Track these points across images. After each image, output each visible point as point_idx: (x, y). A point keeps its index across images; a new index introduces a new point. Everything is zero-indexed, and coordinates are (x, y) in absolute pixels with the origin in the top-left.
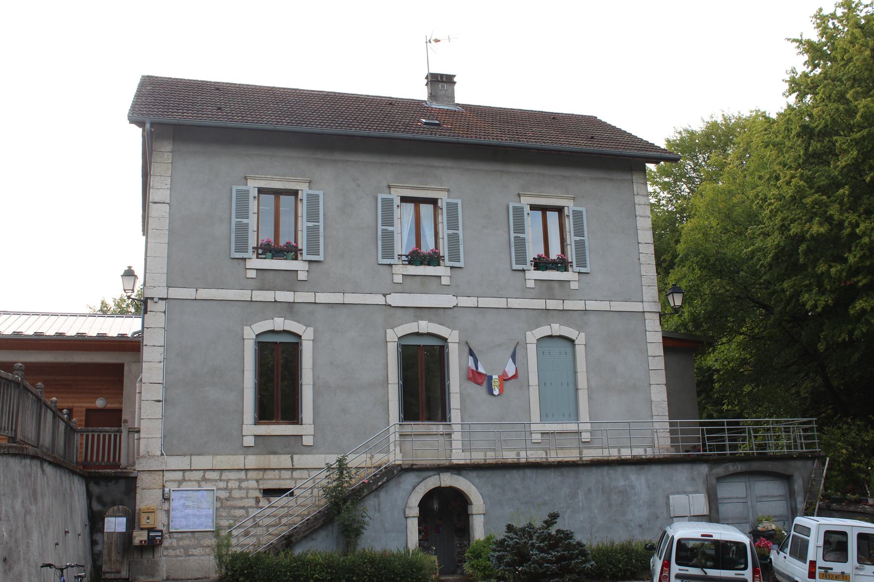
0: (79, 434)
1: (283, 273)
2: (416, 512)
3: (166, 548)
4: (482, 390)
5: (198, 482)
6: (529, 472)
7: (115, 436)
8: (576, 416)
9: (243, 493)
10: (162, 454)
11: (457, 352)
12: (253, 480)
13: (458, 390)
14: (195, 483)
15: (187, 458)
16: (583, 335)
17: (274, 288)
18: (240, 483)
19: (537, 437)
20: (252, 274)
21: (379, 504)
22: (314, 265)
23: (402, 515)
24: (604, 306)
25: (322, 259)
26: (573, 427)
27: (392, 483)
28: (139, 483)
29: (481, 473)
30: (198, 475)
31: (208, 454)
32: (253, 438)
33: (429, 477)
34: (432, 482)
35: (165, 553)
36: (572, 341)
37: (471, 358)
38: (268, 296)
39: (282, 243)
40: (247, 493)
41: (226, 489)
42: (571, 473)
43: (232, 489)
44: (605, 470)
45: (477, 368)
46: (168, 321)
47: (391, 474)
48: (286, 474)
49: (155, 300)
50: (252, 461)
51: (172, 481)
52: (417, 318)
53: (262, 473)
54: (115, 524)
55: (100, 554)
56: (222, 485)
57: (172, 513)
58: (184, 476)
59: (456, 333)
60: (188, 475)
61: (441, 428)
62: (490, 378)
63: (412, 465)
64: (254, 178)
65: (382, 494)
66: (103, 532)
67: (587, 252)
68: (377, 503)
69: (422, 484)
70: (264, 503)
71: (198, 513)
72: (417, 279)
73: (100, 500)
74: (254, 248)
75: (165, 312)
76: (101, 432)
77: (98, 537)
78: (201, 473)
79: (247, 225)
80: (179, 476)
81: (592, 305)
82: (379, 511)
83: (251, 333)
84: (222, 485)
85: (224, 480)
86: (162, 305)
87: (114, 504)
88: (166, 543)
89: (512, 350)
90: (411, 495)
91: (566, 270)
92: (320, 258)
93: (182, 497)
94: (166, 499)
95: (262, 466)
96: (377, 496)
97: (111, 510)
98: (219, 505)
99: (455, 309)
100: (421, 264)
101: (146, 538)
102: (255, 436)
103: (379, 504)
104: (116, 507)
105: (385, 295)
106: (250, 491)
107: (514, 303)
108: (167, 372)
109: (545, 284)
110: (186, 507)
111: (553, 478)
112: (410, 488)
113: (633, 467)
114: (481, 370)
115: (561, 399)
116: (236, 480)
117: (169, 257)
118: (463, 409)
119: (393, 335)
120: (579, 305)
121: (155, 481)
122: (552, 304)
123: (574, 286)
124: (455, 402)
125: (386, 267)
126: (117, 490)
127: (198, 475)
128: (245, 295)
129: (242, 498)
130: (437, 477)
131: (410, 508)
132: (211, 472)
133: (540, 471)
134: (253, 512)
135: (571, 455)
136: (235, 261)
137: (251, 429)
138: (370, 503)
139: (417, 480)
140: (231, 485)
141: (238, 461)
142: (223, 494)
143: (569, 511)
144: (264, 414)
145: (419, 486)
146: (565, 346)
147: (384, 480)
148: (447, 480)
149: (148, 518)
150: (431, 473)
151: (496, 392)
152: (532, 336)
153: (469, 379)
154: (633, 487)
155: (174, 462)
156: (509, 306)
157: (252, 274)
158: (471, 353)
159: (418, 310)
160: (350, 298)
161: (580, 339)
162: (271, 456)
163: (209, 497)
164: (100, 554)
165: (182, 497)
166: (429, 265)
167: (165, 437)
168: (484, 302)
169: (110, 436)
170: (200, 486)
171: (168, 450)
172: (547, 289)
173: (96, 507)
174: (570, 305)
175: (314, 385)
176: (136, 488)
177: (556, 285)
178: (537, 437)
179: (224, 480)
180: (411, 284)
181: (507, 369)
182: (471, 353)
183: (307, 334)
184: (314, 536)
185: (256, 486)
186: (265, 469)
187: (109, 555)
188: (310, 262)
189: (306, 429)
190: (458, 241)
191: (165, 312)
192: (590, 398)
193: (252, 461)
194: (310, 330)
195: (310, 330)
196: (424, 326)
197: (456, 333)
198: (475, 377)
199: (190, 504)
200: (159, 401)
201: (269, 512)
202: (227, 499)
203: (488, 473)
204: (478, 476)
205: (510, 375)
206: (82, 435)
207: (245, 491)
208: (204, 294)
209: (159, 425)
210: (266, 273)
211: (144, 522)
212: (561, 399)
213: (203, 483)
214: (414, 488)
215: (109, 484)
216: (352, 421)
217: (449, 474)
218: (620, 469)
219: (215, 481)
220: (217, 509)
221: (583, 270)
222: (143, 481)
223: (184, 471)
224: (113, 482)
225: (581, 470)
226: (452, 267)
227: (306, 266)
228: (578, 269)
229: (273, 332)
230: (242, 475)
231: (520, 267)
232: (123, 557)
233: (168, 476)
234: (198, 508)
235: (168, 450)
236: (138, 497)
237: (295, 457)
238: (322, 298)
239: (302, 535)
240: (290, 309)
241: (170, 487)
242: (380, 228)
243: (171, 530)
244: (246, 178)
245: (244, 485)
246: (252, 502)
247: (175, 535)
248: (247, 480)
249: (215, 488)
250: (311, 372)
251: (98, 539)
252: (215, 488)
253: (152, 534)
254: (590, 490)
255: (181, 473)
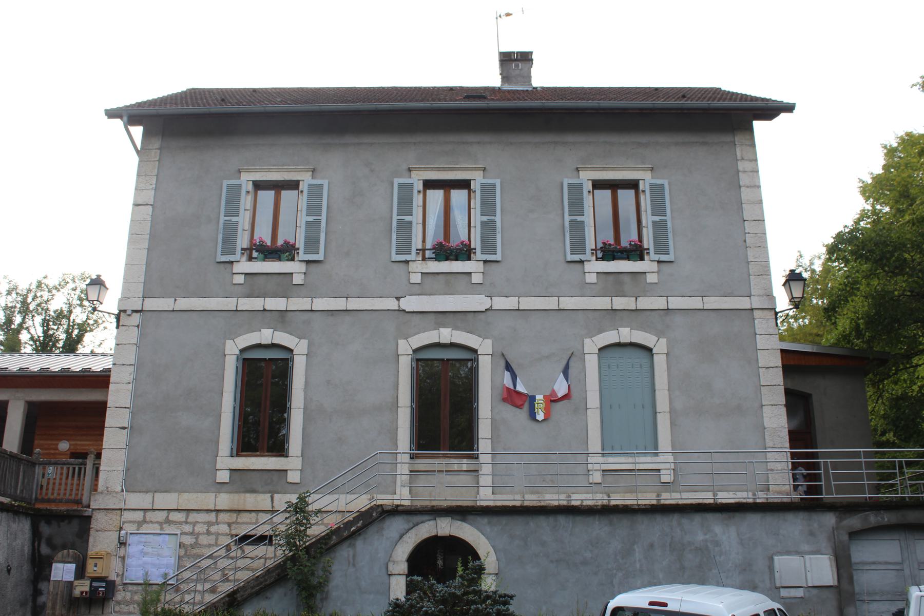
0: (41, 467)
1: (276, 276)
2: (403, 567)
3: (119, 603)
4: (521, 415)
5: (161, 524)
6: (562, 520)
7: (80, 469)
8: (653, 448)
9: (211, 540)
10: (122, 491)
11: (489, 366)
12: (224, 523)
13: (489, 415)
14: (157, 526)
15: (150, 495)
16: (663, 341)
17: (264, 295)
18: (209, 527)
19: (597, 477)
20: (240, 279)
21: (354, 556)
22: (313, 267)
23: (384, 570)
24: (695, 303)
25: (322, 258)
26: (646, 462)
27: (373, 529)
28: (94, 524)
29: (495, 519)
30: (161, 516)
31: (175, 491)
32: (228, 472)
33: (422, 522)
34: (427, 529)
35: (117, 609)
36: (650, 350)
37: (507, 375)
38: (256, 304)
39: (280, 242)
40: (217, 539)
41: (192, 534)
42: (623, 525)
43: (199, 534)
44: (675, 519)
45: (515, 386)
46: (142, 336)
47: (374, 517)
48: (265, 517)
49: (129, 312)
50: (224, 500)
51: (130, 522)
52: (438, 326)
53: (235, 515)
54: (63, 571)
55: (44, 606)
56: (188, 528)
57: (128, 561)
58: (144, 516)
59: (488, 342)
60: (149, 515)
61: (465, 464)
62: (533, 399)
63: (397, 506)
64: (248, 171)
65: (359, 543)
66: (49, 580)
67: (670, 236)
68: (351, 553)
69: (413, 531)
70: (235, 552)
71: (157, 562)
72: (441, 276)
73: (50, 543)
74: (242, 249)
75: (138, 326)
76: (64, 464)
77: (43, 586)
78: (165, 514)
79: (237, 223)
80: (139, 516)
81: (676, 303)
82: (354, 565)
83: (233, 348)
84: (188, 528)
85: (190, 523)
86: (136, 318)
87: (64, 547)
88: (119, 596)
89: (564, 363)
90: (399, 545)
91: (642, 259)
92: (320, 257)
93: (140, 542)
94: (122, 544)
95: (236, 508)
96: (353, 546)
97: (60, 555)
98: (182, 553)
99: (488, 312)
100: (447, 259)
101: (87, 589)
102: (231, 470)
103: (354, 556)
104: (66, 551)
105: (398, 299)
106: (220, 537)
107: (568, 303)
108: (136, 395)
109: (611, 278)
110: (145, 554)
111: (598, 528)
112: (397, 536)
113: (718, 515)
114: (520, 388)
115: (630, 424)
116: (204, 523)
117: (148, 264)
118: (495, 439)
119: (406, 348)
120: (659, 303)
121: (111, 522)
122: (620, 303)
123: (652, 278)
124: (484, 429)
125: (401, 264)
126: (69, 530)
127: (161, 516)
128: (229, 304)
129: (210, 546)
130: (432, 523)
131: (394, 562)
132: (176, 513)
133: (579, 519)
134: (223, 563)
135: (648, 498)
136: (222, 265)
137: (227, 462)
138: (344, 552)
139: (406, 526)
140: (200, 528)
141: (208, 500)
142: (188, 540)
143: (620, 574)
144: (247, 443)
145: (408, 535)
146: (639, 357)
147: (359, 525)
148: (445, 527)
149: (96, 566)
150: (426, 517)
151: (540, 416)
152: (592, 345)
153: (504, 400)
154: (717, 544)
155: (136, 500)
156: (561, 307)
157: (240, 279)
158: (508, 367)
159: (441, 316)
160: (355, 304)
161: (660, 347)
162: (248, 495)
163: (172, 543)
164: (44, 606)
165: (140, 542)
166: (457, 259)
167: (128, 470)
168: (527, 303)
169: (74, 469)
170: (162, 529)
171: (130, 486)
172: (614, 284)
173: (45, 550)
174: (645, 303)
175: (305, 409)
176: (89, 529)
177: (627, 279)
178: (597, 477)
179: (190, 523)
180: (431, 284)
181: (556, 388)
182: (508, 367)
183: (300, 347)
184: (268, 594)
185: (228, 531)
186: (240, 511)
187: (53, 608)
188: (308, 262)
189: (292, 463)
190: (495, 229)
191: (138, 326)
192: (673, 424)
193: (224, 500)
194: (304, 343)
195: (304, 343)
196: (446, 335)
197: (488, 342)
198: (512, 397)
199: (150, 550)
200: (124, 428)
201: (241, 563)
202: (192, 546)
203: (504, 520)
204: (489, 523)
205: (560, 395)
206: (62, 468)
207: (214, 537)
208: (184, 304)
209: (122, 455)
210: (256, 278)
211: (91, 570)
212: (630, 424)
213: (165, 526)
214: (401, 537)
215: (62, 524)
216: (354, 452)
217: (448, 519)
218: (698, 518)
219: (180, 523)
220: (180, 558)
221: (664, 258)
222: (99, 521)
223: (145, 510)
224: (66, 521)
225: (639, 518)
226: (485, 262)
227: (302, 267)
228: (657, 257)
229: (259, 346)
230: (212, 517)
231: (576, 257)
232: (69, 611)
233: (127, 516)
234: (158, 555)
235: (130, 486)
236: (91, 540)
237: (276, 496)
238: (321, 304)
239: (249, 591)
240: (281, 319)
241: (129, 528)
242: (395, 218)
243: (125, 582)
244: (239, 172)
245: (213, 529)
246: (223, 552)
247: (130, 588)
248: (217, 523)
249: (179, 532)
250: (302, 393)
251: (43, 588)
252: (179, 532)
253: (95, 584)
254: (652, 546)
255: (142, 513)
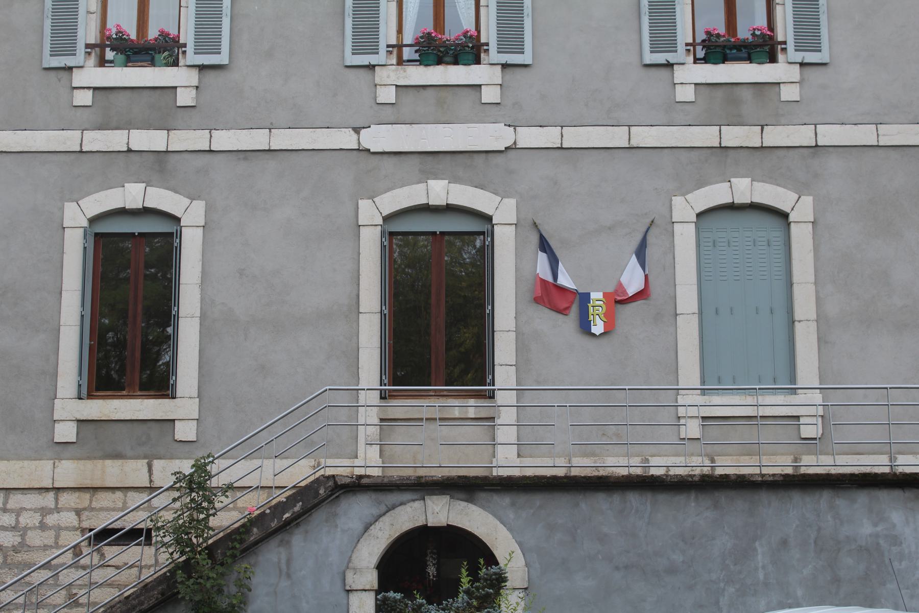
2: (371, 578)
4: (568, 324)
6: (634, 499)
8: (789, 381)
9: (48, 538)
11: (512, 243)
13: (512, 325)
16: (807, 201)
17: (128, 125)
18: (43, 516)
19: (693, 429)
20: (84, 98)
22: (211, 76)
24: (864, 135)
25: (226, 61)
26: (775, 404)
27: (319, 516)
29: (522, 498)
33: (402, 504)
34: (410, 515)
36: (784, 216)
37: (542, 258)
38: (115, 140)
39: (153, 33)
40: (57, 537)
41: (14, 528)
42: (736, 508)
43: (26, 529)
44: (825, 497)
45: (555, 277)
48: (139, 498)
50: (69, 472)
52: (425, 176)
53: (87, 496)
59: (511, 203)
61: (472, 408)
62: (585, 298)
63: (360, 477)
65: (297, 539)
67: (823, 19)
68: (284, 557)
69: (386, 519)
72: (430, 92)
74: (87, 46)
81: (830, 135)
82: (289, 576)
83: (76, 216)
89: (638, 237)
90: (364, 542)
91: (773, 59)
92: (222, 59)
96: (287, 544)
99: (512, 154)
100: (439, 62)
102: (79, 421)
103: (289, 562)
105: (357, 130)
106: (63, 534)
107: (645, 136)
109: (719, 93)
111: (694, 512)
113: (897, 494)
114: (564, 280)
115: (751, 340)
116: (35, 510)
118: (521, 365)
119: (371, 213)
120: (802, 136)
122: (734, 136)
123: (789, 93)
124: (504, 350)
125: (362, 72)
128: (69, 140)
129: (46, 548)
130: (418, 504)
133: (662, 497)
134: (68, 577)
135: (779, 464)
136: (52, 74)
137: (71, 407)
138: (271, 555)
139: (375, 511)
140: (26, 519)
141: (42, 472)
143: (731, 590)
144: (103, 379)
145: (378, 525)
146: (768, 227)
148: (440, 512)
150: (407, 496)
151: (598, 328)
152: (686, 208)
153: (537, 300)
154: (895, 540)
156: (634, 143)
157: (84, 98)
158: (544, 245)
159: (430, 158)
160: (283, 139)
161: (802, 210)
162: (108, 462)
166: (456, 63)
168: (575, 137)
172: (725, 103)
174: (776, 136)
175: (203, 317)
177: (746, 94)
178: (693, 429)
180: (413, 104)
181: (624, 280)
182: (544, 245)
183: (191, 214)
185: (76, 523)
186: (95, 489)
188: (202, 68)
189: (183, 408)
190: (521, 10)
192: (822, 341)
193: (69, 472)
194: (199, 207)
195: (199, 207)
196: (439, 191)
197: (511, 203)
198: (551, 296)
201: (99, 576)
202: (15, 549)
203: (538, 499)
204: (513, 504)
205: (631, 291)
210: (113, 96)
212: (751, 340)
214: (367, 528)
217: (445, 499)
218: (863, 497)
221: (811, 57)
225: (764, 496)
226: (505, 66)
227: (193, 77)
228: (799, 57)
230: (49, 500)
231: (660, 58)
237: (157, 464)
238: (225, 140)
240: (158, 166)
245: (51, 520)
246: (68, 558)
248: (58, 510)
254: (784, 543)
